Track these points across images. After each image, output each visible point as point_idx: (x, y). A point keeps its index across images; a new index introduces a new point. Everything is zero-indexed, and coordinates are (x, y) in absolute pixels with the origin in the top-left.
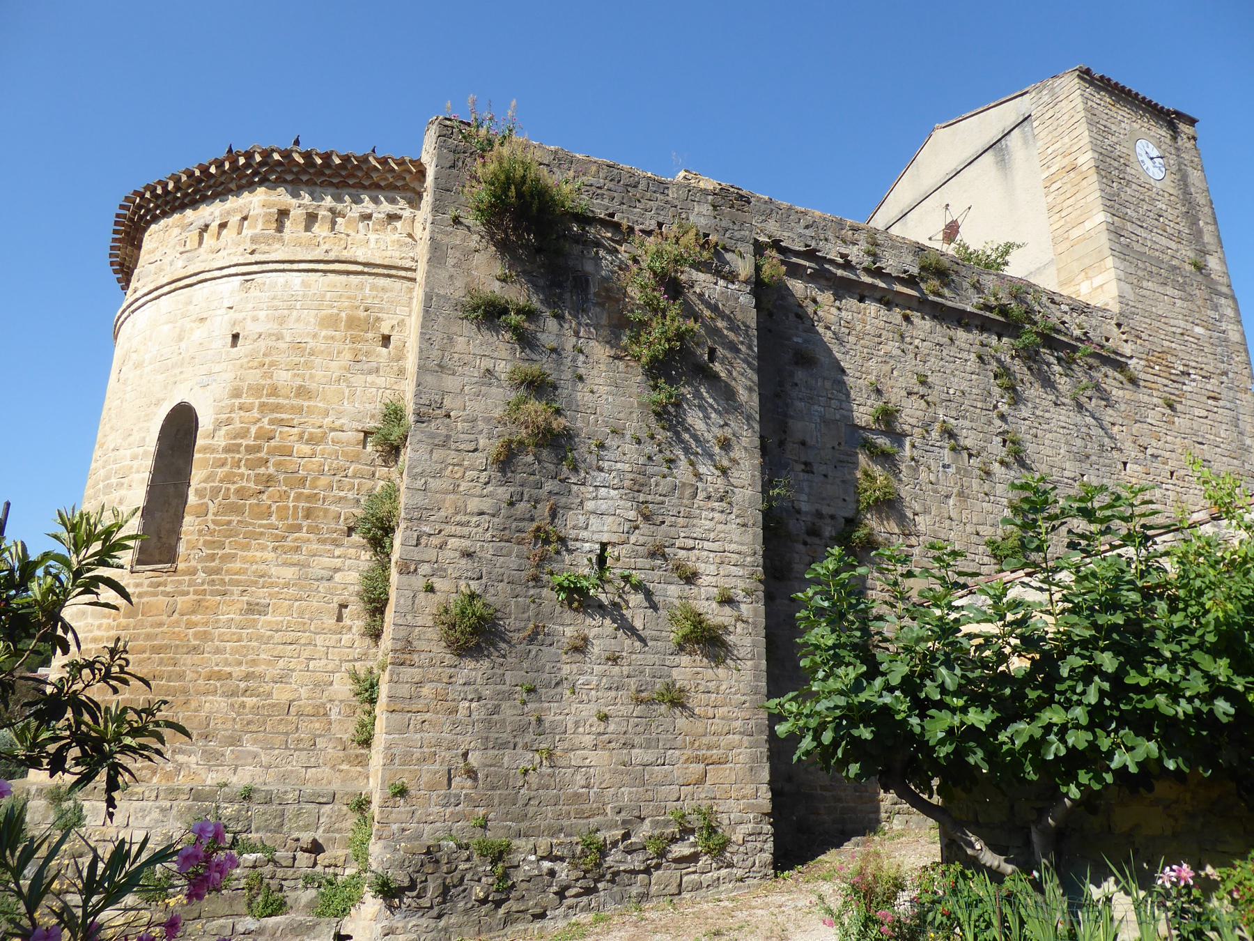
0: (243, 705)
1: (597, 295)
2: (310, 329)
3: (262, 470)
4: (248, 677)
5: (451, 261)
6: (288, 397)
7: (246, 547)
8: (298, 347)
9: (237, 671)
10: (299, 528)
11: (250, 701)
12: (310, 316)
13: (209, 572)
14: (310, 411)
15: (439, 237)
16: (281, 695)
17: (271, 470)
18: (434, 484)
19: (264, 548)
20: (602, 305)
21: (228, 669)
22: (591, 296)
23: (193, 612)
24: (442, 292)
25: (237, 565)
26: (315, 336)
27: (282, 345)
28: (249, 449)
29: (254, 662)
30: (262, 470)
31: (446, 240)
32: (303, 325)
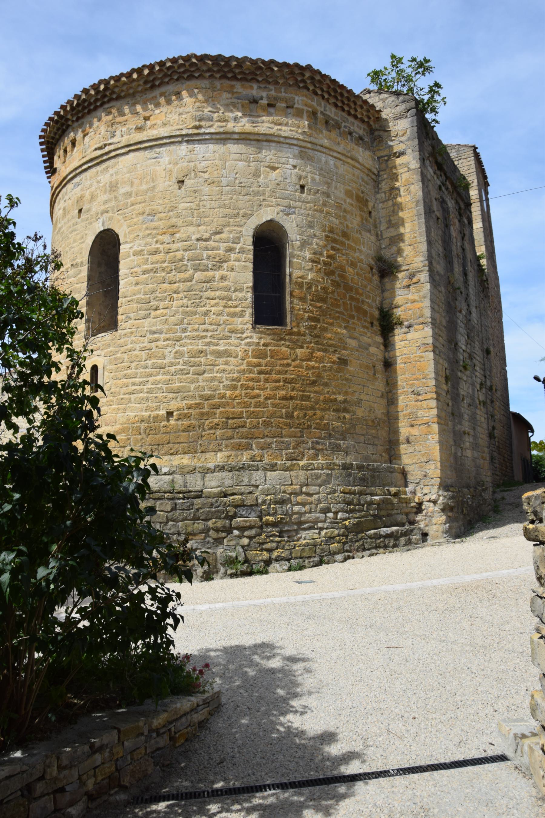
0: (344, 418)
4: (345, 401)
6: (338, 235)
9: (340, 398)
11: (347, 416)
14: (350, 247)
16: (360, 412)
21: (334, 397)
28: (325, 264)
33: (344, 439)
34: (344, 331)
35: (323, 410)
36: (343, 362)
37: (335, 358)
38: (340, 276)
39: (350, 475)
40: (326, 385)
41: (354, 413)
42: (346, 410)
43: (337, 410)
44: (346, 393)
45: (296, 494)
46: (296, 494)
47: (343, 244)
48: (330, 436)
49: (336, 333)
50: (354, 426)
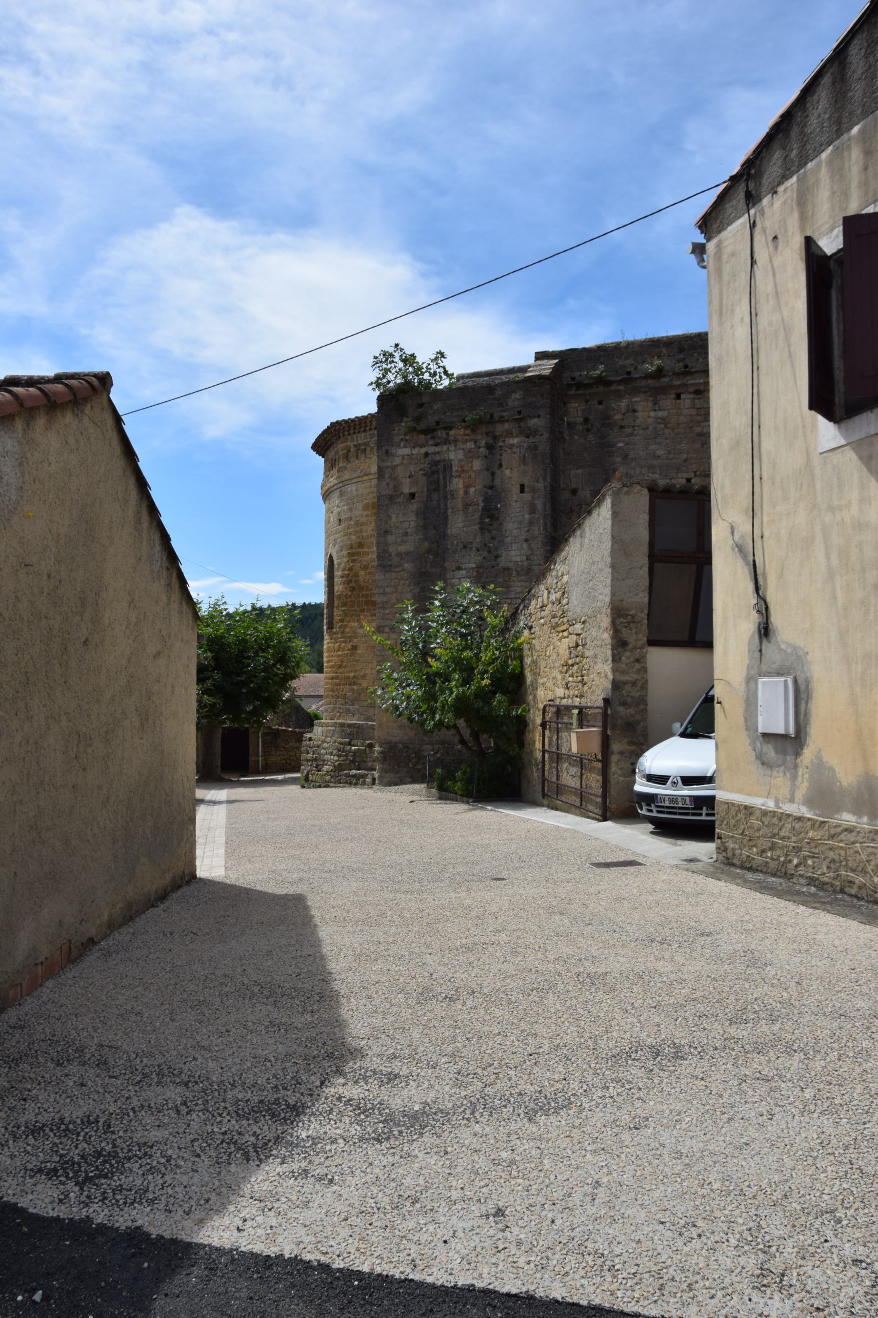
1: (456, 471)
2: (361, 512)
3: (351, 585)
4: (354, 677)
5: (387, 475)
7: (349, 621)
8: (358, 524)
9: (352, 675)
10: (363, 611)
11: (355, 687)
12: (359, 506)
13: (342, 633)
15: (380, 465)
17: (353, 584)
18: (388, 590)
19: (354, 621)
20: (459, 476)
22: (454, 473)
23: (339, 651)
24: (384, 493)
25: (347, 630)
26: (362, 516)
27: (352, 523)
29: (355, 671)
30: (351, 585)
31: (385, 464)
32: (358, 512)
33: (353, 705)
34: (356, 624)
35: (344, 685)
36: (355, 648)
37: (349, 646)
38: (355, 582)
39: (343, 731)
40: (345, 667)
41: (360, 684)
42: (355, 684)
43: (350, 684)
44: (355, 671)
45: (324, 742)
46: (324, 742)
47: (358, 554)
48: (346, 703)
49: (351, 627)
50: (359, 694)
